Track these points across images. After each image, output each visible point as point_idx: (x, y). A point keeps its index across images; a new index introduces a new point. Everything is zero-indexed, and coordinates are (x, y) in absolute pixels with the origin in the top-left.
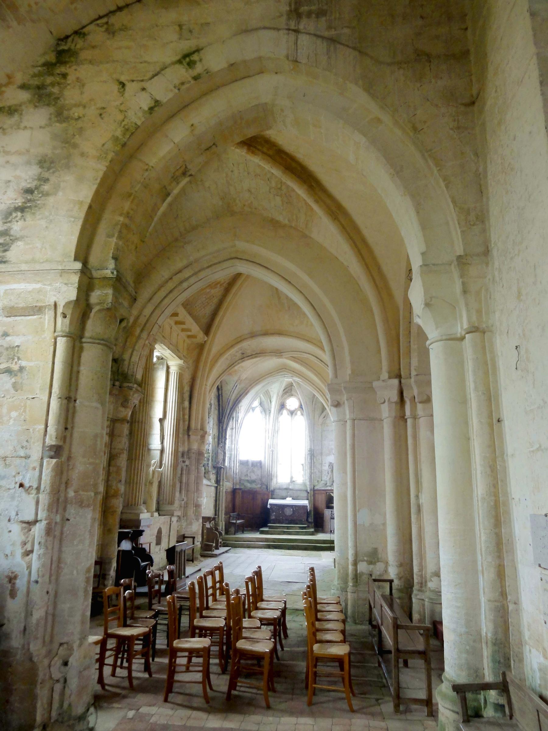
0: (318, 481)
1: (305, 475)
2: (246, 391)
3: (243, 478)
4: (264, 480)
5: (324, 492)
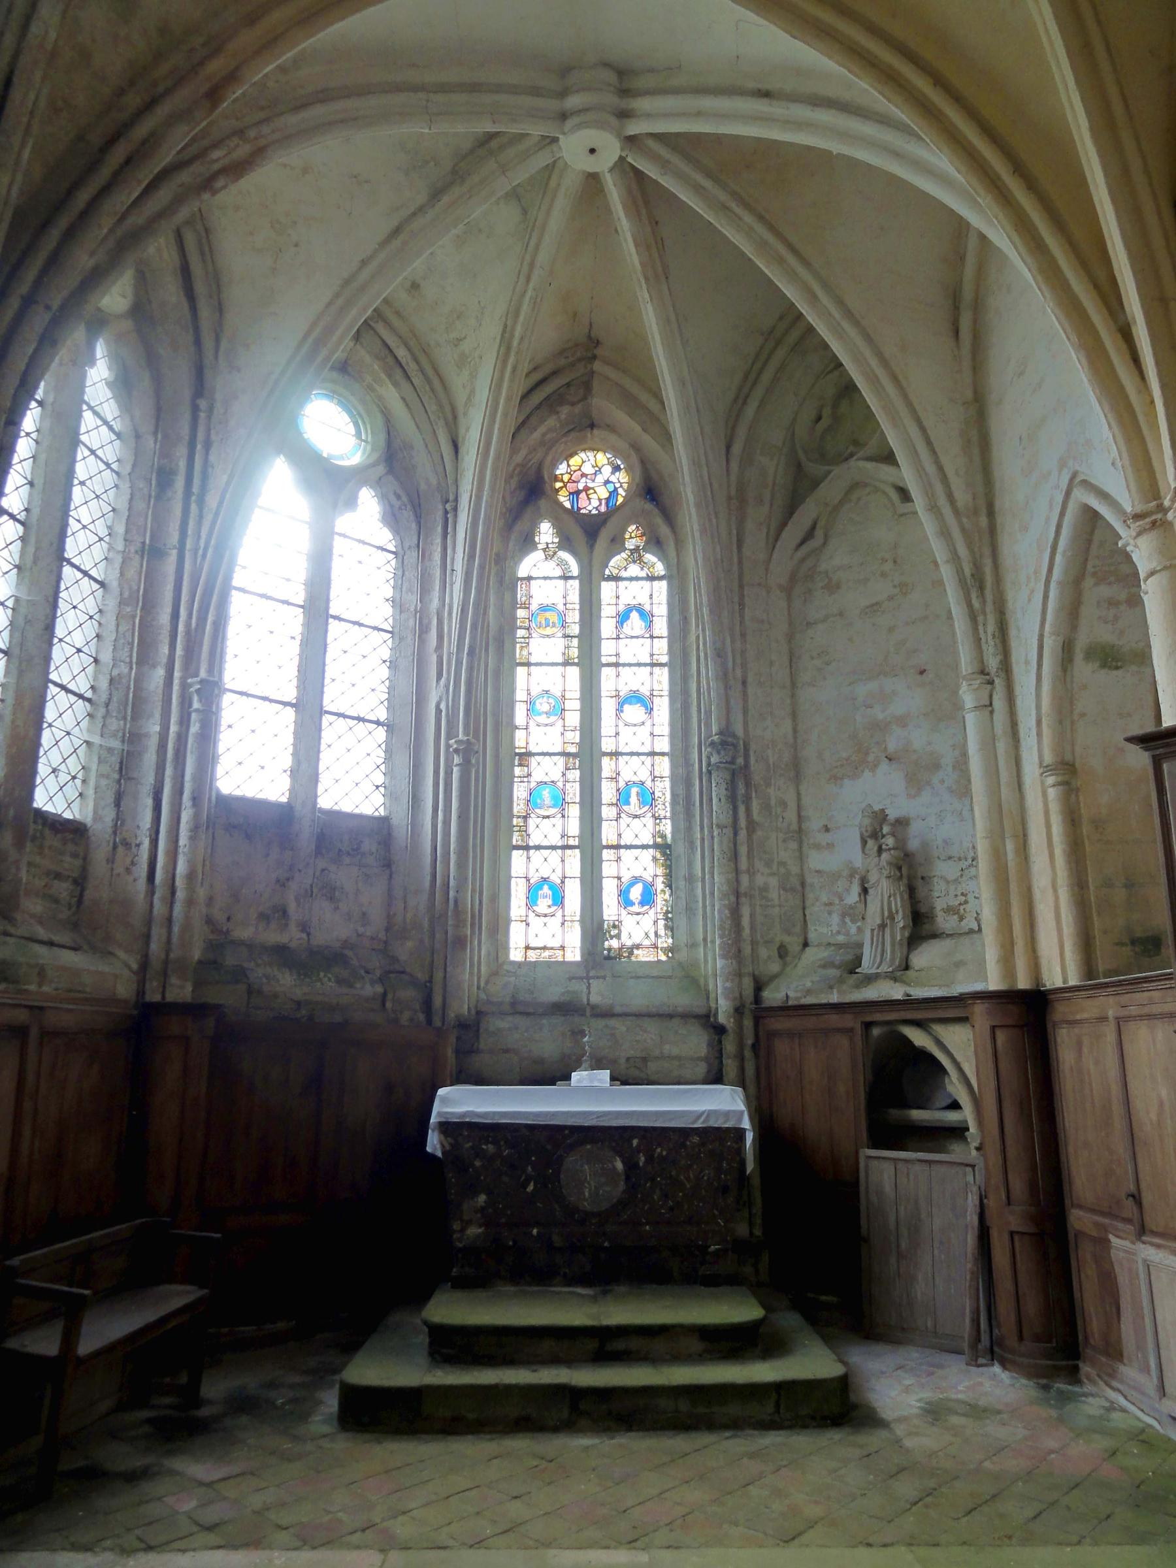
0: (782, 952)
1: (690, 911)
2: (216, 67)
3: (243, 933)
4: (404, 950)
5: (848, 1021)
